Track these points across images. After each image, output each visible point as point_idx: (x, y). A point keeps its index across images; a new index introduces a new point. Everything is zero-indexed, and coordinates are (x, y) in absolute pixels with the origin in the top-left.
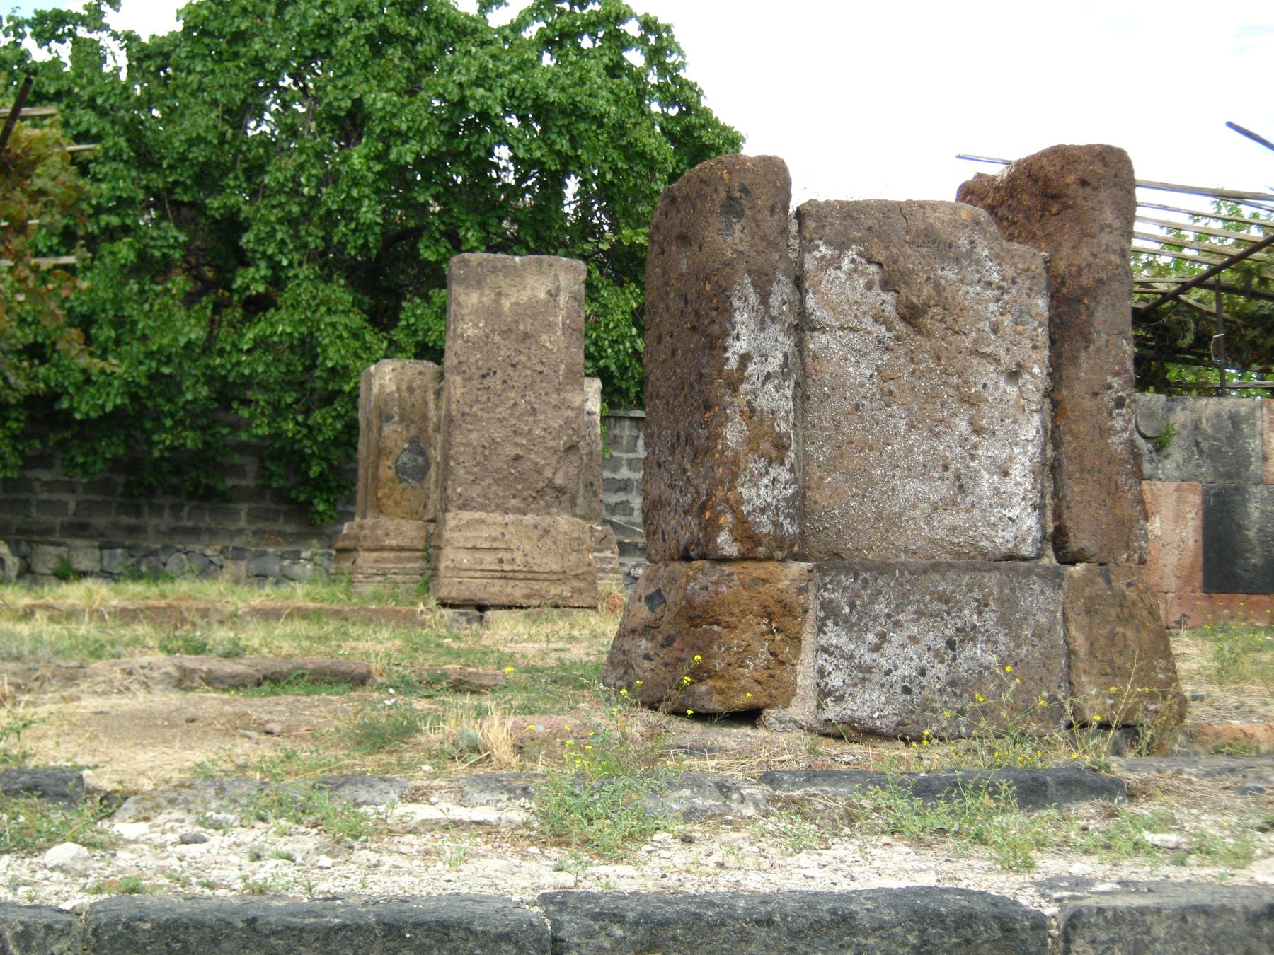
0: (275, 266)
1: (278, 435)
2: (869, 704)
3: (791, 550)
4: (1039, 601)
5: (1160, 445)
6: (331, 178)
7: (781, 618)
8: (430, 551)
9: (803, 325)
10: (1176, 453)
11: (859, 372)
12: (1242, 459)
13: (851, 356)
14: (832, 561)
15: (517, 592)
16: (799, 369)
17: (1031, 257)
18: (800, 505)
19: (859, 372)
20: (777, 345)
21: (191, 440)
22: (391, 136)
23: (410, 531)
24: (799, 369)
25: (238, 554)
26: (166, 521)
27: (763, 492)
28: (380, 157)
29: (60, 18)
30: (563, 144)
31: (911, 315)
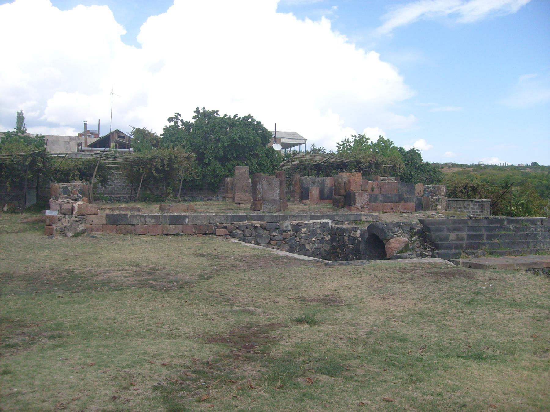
0: (209, 159)
1: (211, 181)
2: (267, 210)
3: (261, 200)
4: (278, 203)
5: (314, 183)
6: (216, 147)
7: (261, 204)
8: (234, 198)
9: (262, 185)
10: (316, 184)
11: (266, 188)
12: (324, 184)
13: (265, 187)
14: (264, 200)
15: (243, 202)
16: (262, 187)
17: (278, 179)
18: (262, 197)
19: (266, 188)
20: (261, 186)
21: (200, 183)
22: (224, 142)
23: (231, 196)
24: (262, 187)
25: (205, 197)
26: (196, 193)
27: (260, 196)
28: (223, 145)
29: (173, 118)
30: (246, 142)
31: (270, 184)
